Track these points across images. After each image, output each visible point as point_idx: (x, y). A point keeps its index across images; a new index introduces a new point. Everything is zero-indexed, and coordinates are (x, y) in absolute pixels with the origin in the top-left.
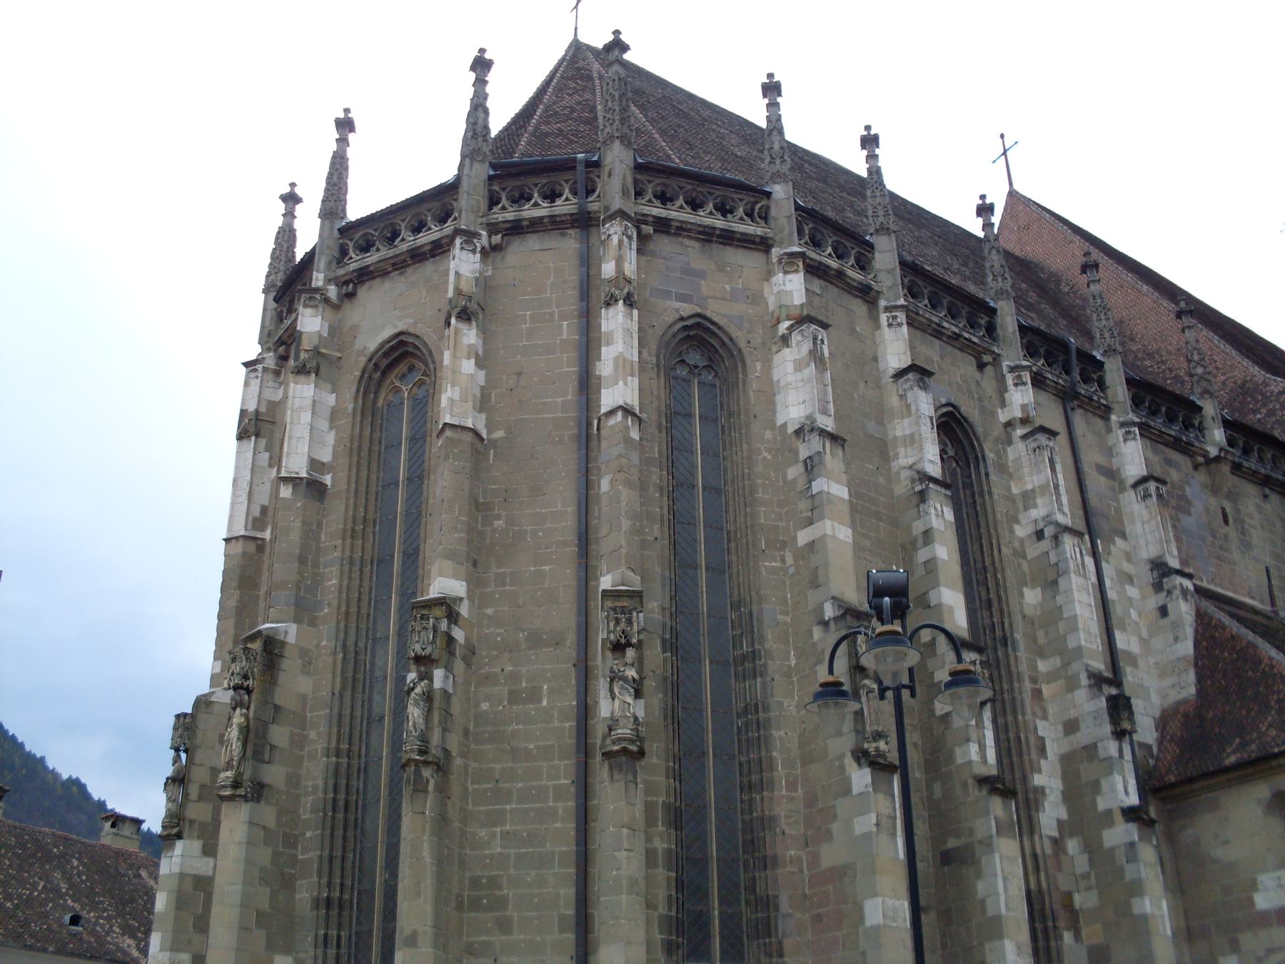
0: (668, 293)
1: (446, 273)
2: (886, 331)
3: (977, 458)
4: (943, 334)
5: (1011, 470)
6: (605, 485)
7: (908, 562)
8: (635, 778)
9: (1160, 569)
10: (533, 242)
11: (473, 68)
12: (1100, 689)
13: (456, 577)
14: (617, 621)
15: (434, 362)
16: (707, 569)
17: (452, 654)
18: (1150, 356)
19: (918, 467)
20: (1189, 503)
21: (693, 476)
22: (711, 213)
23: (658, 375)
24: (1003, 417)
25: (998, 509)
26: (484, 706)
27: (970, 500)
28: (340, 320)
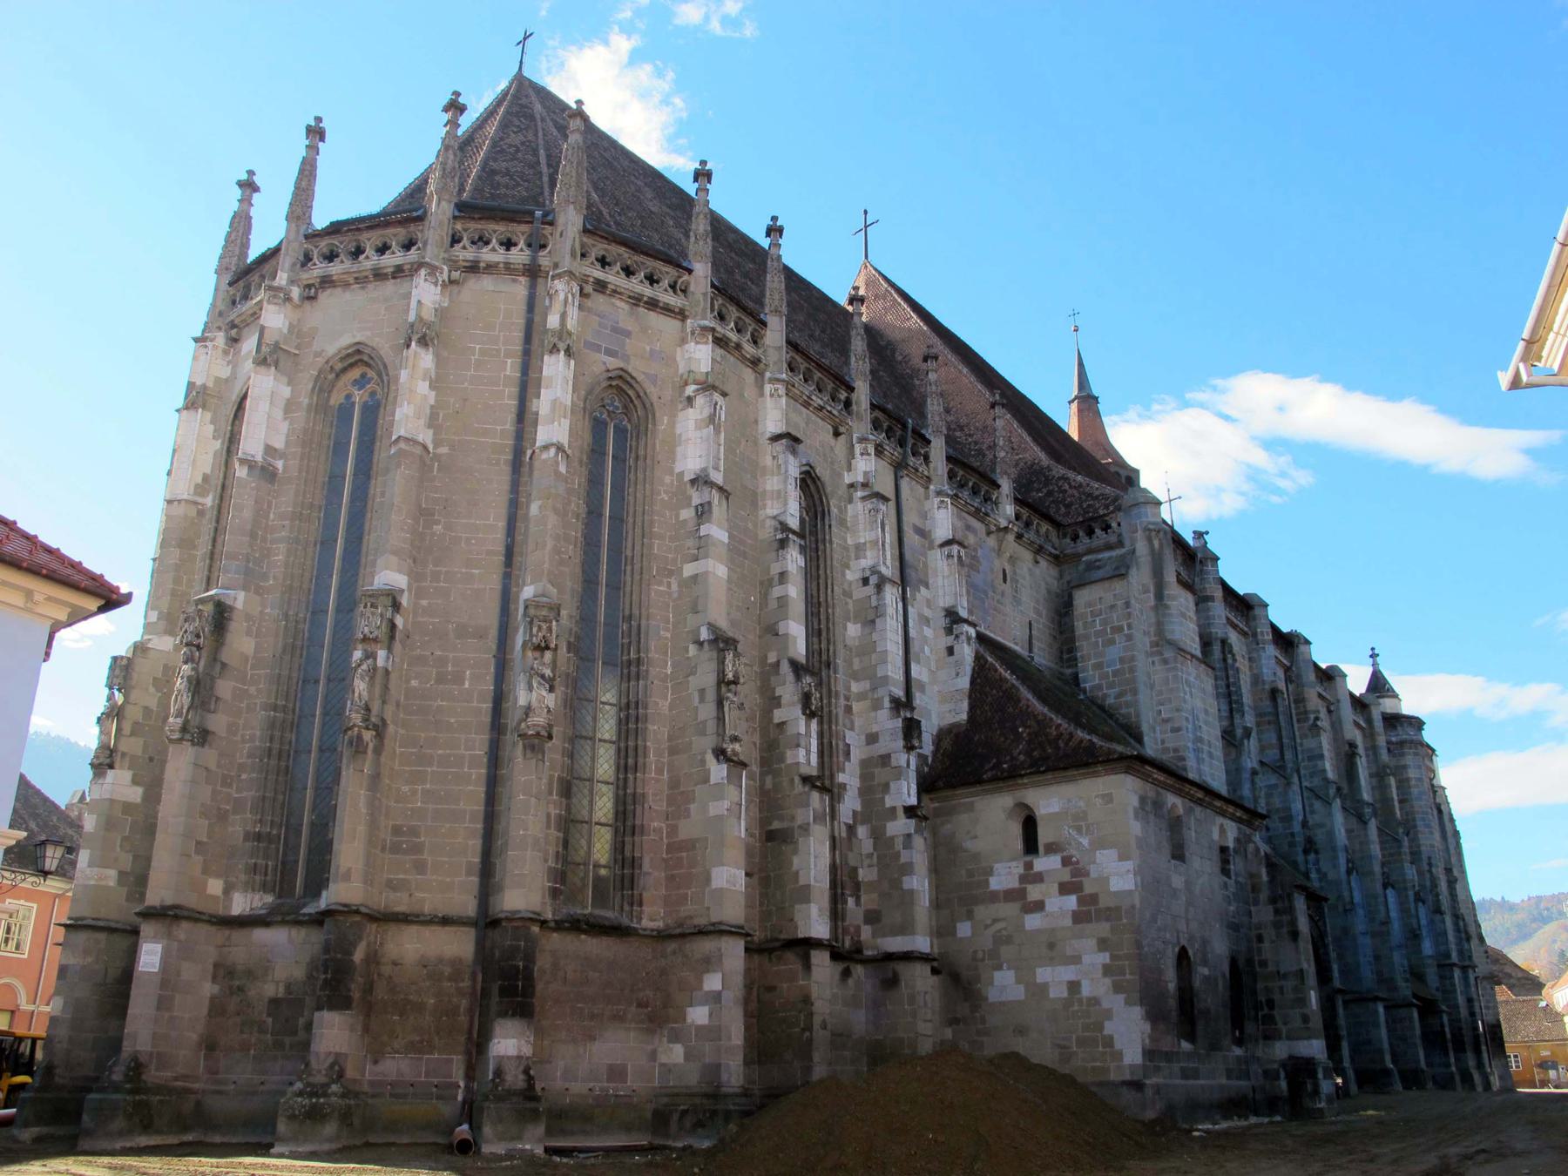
0: (599, 346)
1: (408, 296)
2: (769, 402)
3: (823, 510)
4: (810, 405)
5: (849, 524)
6: (534, 509)
7: (765, 597)
8: (544, 757)
9: (953, 617)
10: (487, 283)
11: (446, 109)
12: (898, 712)
13: (400, 572)
14: (540, 628)
15: (388, 375)
16: (607, 585)
17: (392, 637)
18: (961, 428)
19: (782, 518)
20: (978, 561)
21: (602, 505)
22: (641, 282)
23: (584, 418)
24: (848, 479)
25: (835, 556)
26: (414, 683)
27: (814, 546)
28: (299, 320)
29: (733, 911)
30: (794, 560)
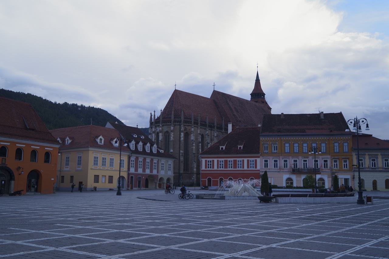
6: (181, 145)
10: (176, 126)
24: (206, 133)
29: (195, 172)
30: (200, 144)
